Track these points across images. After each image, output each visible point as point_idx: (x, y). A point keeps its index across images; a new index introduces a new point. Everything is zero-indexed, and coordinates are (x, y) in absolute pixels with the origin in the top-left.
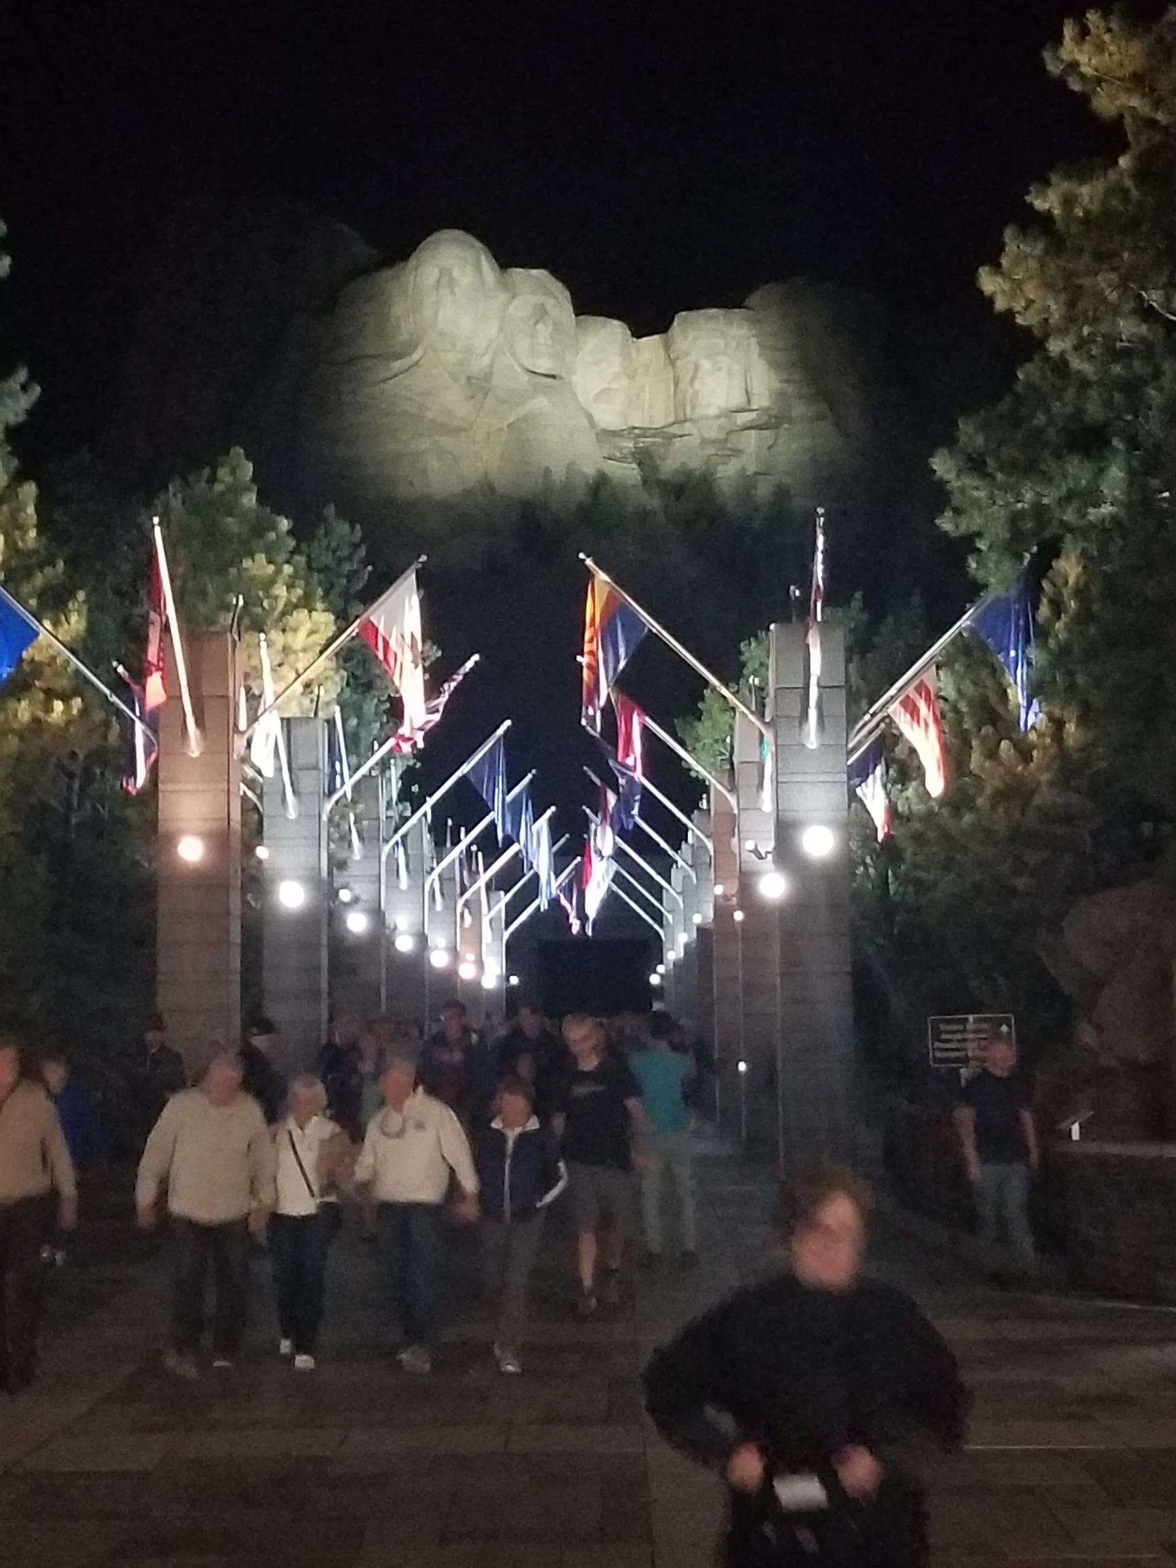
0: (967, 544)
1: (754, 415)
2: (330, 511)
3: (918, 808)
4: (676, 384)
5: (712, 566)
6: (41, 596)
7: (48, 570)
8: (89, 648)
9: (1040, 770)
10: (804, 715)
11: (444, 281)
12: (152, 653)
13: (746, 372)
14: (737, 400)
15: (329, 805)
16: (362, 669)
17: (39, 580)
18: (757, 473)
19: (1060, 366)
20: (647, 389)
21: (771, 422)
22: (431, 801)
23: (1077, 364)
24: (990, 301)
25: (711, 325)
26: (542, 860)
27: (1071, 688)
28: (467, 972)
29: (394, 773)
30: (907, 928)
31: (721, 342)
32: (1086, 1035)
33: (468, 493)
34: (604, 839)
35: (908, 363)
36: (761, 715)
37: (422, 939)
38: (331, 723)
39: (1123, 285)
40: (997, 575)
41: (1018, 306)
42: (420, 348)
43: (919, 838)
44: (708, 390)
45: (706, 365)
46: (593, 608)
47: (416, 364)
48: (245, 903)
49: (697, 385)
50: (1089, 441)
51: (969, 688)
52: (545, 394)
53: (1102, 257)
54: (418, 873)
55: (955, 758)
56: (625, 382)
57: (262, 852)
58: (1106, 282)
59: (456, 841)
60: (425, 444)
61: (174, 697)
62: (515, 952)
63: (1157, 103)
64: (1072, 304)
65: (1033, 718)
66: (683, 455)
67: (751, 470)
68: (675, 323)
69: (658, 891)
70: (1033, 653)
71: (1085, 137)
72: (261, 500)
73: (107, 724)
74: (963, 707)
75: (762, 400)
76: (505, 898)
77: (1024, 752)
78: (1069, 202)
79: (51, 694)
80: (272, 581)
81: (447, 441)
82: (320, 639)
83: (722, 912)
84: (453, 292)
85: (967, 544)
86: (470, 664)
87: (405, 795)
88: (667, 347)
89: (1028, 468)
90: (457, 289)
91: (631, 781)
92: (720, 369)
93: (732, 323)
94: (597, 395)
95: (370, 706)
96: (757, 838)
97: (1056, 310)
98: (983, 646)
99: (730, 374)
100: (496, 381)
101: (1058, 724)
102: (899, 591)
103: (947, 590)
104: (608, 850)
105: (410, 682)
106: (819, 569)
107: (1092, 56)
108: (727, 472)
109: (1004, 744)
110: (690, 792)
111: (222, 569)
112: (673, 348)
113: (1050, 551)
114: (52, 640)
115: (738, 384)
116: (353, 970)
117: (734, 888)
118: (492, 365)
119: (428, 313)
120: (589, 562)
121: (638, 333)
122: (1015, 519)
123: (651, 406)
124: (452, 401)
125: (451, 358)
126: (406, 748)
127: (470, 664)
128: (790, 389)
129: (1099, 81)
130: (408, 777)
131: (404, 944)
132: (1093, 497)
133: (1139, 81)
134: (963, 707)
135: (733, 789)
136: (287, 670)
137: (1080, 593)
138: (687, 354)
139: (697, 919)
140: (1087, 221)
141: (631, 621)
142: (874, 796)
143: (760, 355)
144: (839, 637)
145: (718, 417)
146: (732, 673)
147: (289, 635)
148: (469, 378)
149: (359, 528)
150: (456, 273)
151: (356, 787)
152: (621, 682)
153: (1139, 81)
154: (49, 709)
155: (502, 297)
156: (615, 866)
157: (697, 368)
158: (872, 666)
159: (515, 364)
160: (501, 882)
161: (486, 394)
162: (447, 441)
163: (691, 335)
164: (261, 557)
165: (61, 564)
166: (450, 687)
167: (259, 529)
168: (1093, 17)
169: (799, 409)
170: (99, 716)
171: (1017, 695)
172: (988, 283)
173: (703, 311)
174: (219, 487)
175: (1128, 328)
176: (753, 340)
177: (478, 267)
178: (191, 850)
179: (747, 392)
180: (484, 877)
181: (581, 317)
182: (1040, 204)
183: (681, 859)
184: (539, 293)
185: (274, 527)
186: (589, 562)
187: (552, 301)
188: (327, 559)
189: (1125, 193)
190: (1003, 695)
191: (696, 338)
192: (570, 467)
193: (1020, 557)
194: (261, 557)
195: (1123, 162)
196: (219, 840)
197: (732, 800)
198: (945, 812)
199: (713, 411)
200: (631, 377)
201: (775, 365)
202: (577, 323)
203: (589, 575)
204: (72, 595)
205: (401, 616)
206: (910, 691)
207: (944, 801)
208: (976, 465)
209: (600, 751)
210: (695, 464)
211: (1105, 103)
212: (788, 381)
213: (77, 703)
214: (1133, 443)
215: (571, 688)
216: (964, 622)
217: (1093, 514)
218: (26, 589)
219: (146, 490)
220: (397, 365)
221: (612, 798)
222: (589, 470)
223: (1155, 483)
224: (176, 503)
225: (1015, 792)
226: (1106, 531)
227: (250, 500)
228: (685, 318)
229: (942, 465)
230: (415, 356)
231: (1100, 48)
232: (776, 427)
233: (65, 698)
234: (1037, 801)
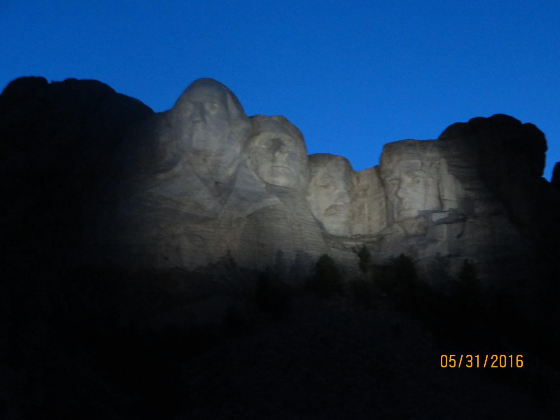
4: (387, 198)
13: (438, 184)
14: (432, 204)
18: (449, 256)
31: (417, 162)
45: (407, 180)
52: (278, 196)
56: (348, 200)
67: (445, 252)
75: (451, 203)
84: (204, 120)
90: (208, 119)
94: (327, 210)
99: (426, 185)
108: (426, 254)
115: (432, 191)
118: (235, 174)
119: (185, 137)
123: (369, 219)
124: (204, 197)
125: (203, 169)
128: (472, 194)
138: (392, 172)
143: (449, 171)
145: (417, 218)
148: (217, 183)
150: (207, 107)
157: (400, 180)
159: (255, 175)
169: (479, 209)
176: (443, 161)
187: (288, 137)
191: (399, 160)
199: (414, 213)
200: (354, 199)
201: (460, 178)
212: (469, 189)
220: (162, 176)
222: (315, 253)
232: (464, 220)
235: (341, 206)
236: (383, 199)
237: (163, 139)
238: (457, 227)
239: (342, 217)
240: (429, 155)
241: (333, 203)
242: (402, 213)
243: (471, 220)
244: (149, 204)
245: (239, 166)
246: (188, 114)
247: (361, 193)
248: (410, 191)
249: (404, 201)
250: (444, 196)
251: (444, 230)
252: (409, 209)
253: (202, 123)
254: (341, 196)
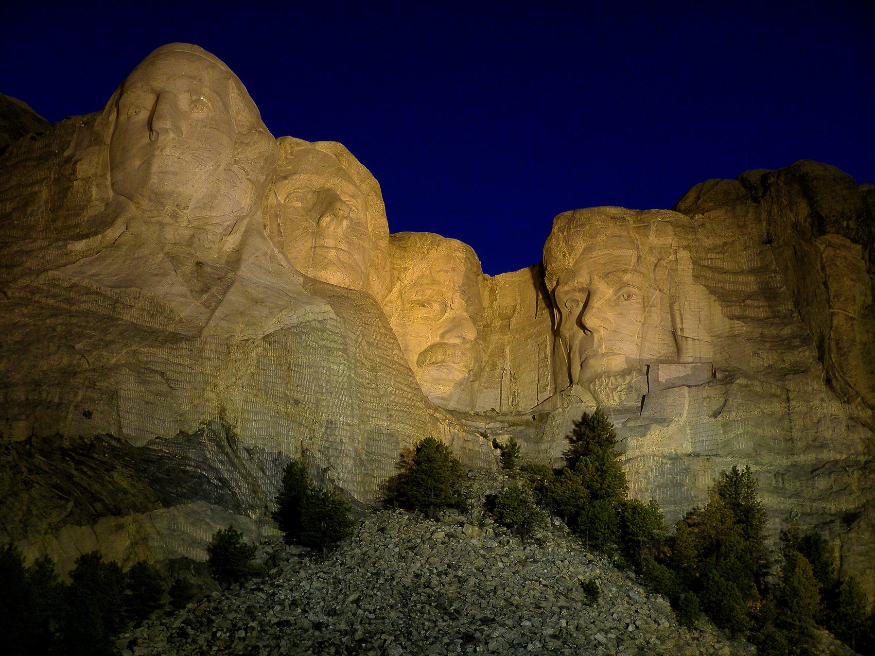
1: (688, 370)
4: (556, 333)
11: (164, 107)
13: (671, 306)
14: (656, 345)
20: (507, 351)
25: (613, 229)
31: (630, 254)
42: (120, 221)
45: (605, 291)
47: (114, 245)
49: (590, 321)
52: (332, 304)
56: (471, 334)
68: (555, 230)
75: (700, 349)
84: (177, 129)
92: (629, 296)
93: (647, 227)
99: (646, 305)
100: (245, 271)
112: (549, 268)
115: (658, 317)
118: (239, 251)
121: (493, 263)
125: (169, 235)
138: (572, 273)
143: (696, 277)
145: (624, 373)
148: (199, 264)
155: (264, 143)
159: (280, 256)
161: (229, 287)
163: (580, 245)
173: (602, 208)
176: (684, 254)
177: (221, 94)
179: (674, 334)
181: (398, 235)
191: (588, 249)
199: (617, 363)
200: (484, 333)
202: (392, 240)
212: (738, 318)
220: (80, 246)
228: (570, 220)
230: (111, 234)
235: (454, 345)
236: (548, 337)
237: (84, 169)
239: (457, 371)
240: (653, 239)
241: (438, 339)
242: (592, 362)
243: (742, 381)
244: (51, 302)
245: (247, 233)
246: (144, 115)
247: (497, 323)
248: (610, 315)
249: (596, 336)
250: (682, 329)
252: (607, 354)
253: (172, 135)
254: (455, 325)
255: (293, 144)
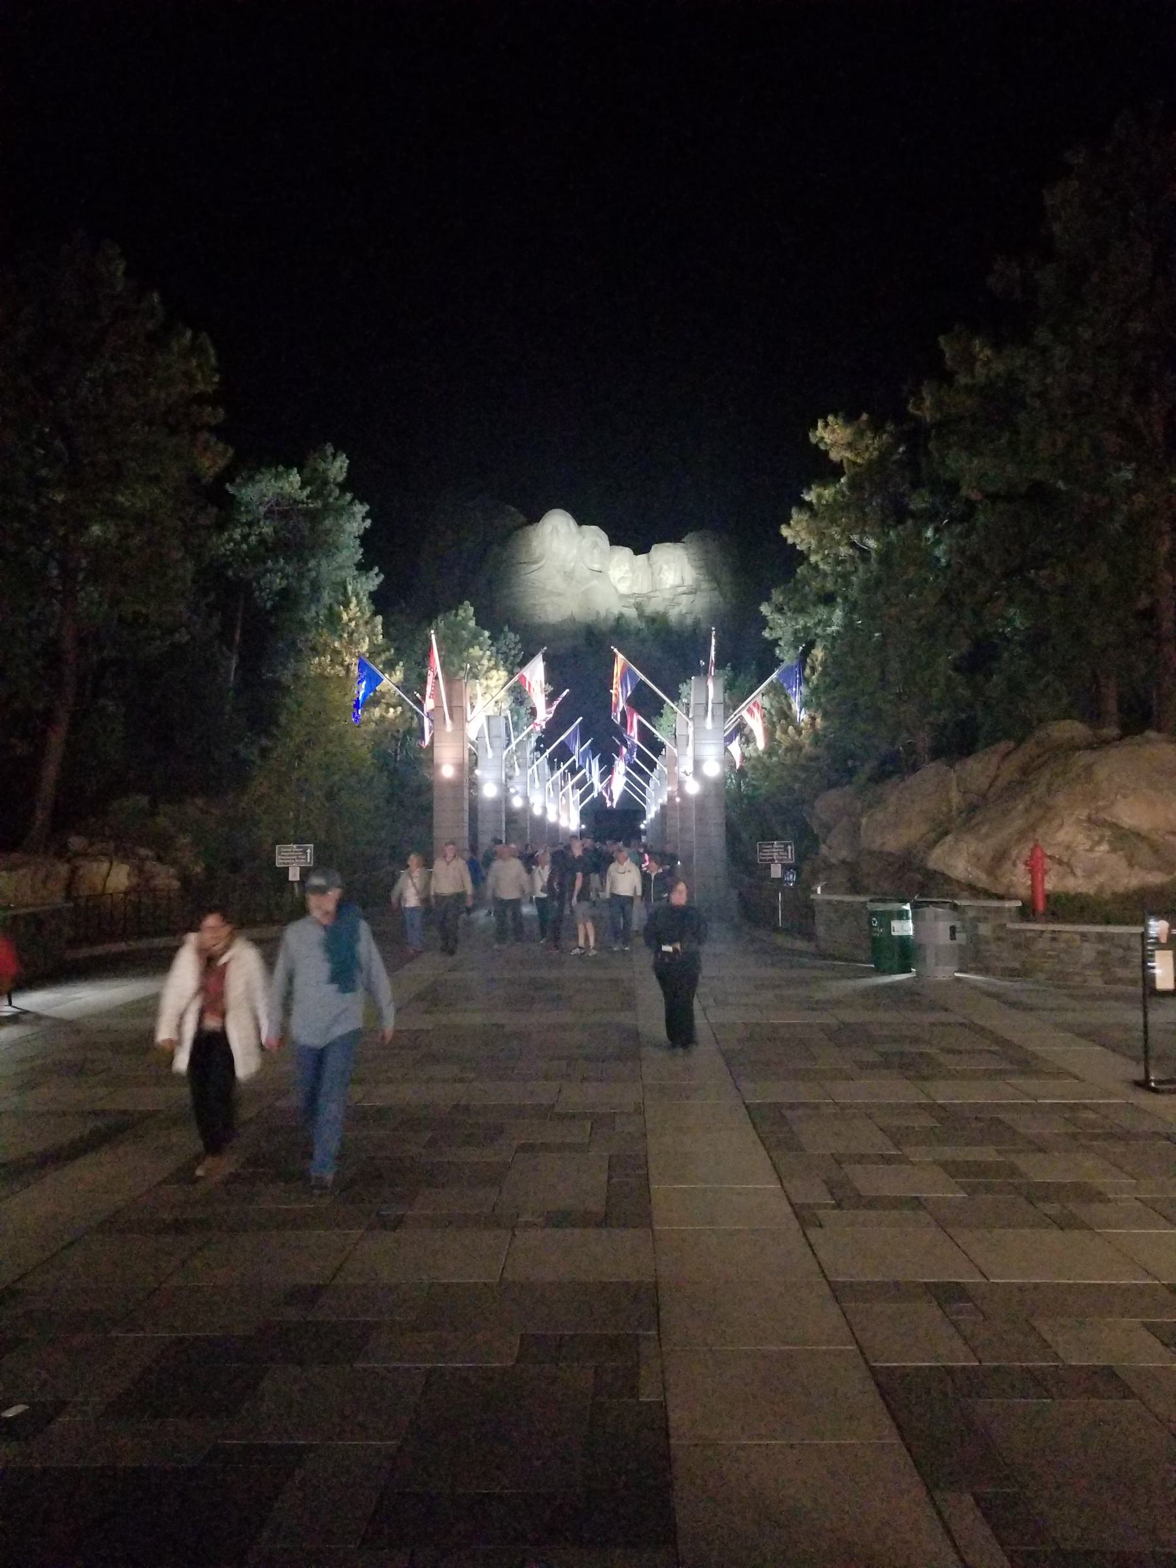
0: (775, 643)
2: (506, 628)
3: (754, 755)
5: (669, 653)
6: (384, 663)
7: (387, 654)
8: (405, 686)
9: (805, 739)
10: (707, 711)
12: (429, 689)
14: (678, 581)
15: (505, 753)
16: (519, 695)
17: (383, 657)
19: (816, 567)
21: (693, 592)
22: (548, 751)
23: (822, 566)
24: (785, 539)
26: (595, 777)
27: (819, 705)
28: (563, 823)
29: (533, 739)
30: (753, 809)
32: (824, 849)
33: (564, 621)
34: (620, 767)
35: (753, 564)
36: (687, 714)
37: (545, 809)
38: (506, 718)
39: (843, 532)
40: (788, 656)
41: (798, 541)
43: (754, 767)
44: (667, 578)
45: (665, 567)
46: (617, 669)
48: (470, 794)
50: (828, 599)
51: (775, 703)
53: (833, 521)
54: (544, 781)
55: (770, 734)
57: (477, 772)
58: (835, 531)
59: (559, 768)
60: (543, 600)
61: (439, 707)
62: (583, 814)
63: (857, 455)
64: (820, 541)
65: (803, 716)
66: (654, 606)
69: (644, 789)
70: (803, 689)
71: (827, 470)
72: (477, 624)
73: (412, 718)
74: (773, 712)
76: (579, 792)
77: (799, 731)
78: (819, 497)
79: (388, 705)
80: (482, 658)
81: (556, 599)
82: (502, 682)
83: (671, 798)
85: (775, 643)
86: (565, 693)
87: (537, 749)
88: (649, 558)
89: (801, 610)
91: (633, 743)
95: (523, 711)
96: (687, 765)
97: (814, 543)
98: (782, 686)
99: (675, 571)
101: (813, 719)
102: (747, 662)
103: (766, 661)
104: (623, 772)
105: (538, 698)
106: (713, 653)
107: (831, 435)
108: (673, 614)
109: (791, 728)
110: (657, 748)
111: (461, 652)
113: (811, 645)
114: (389, 683)
115: (678, 574)
116: (515, 821)
117: (676, 788)
120: (615, 650)
122: (796, 632)
124: (556, 582)
126: (538, 729)
127: (565, 693)
128: (701, 577)
129: (833, 445)
130: (539, 740)
131: (537, 811)
132: (828, 623)
133: (850, 446)
134: (773, 712)
135: (676, 746)
136: (487, 696)
137: (824, 664)
139: (660, 801)
140: (828, 505)
141: (633, 676)
142: (735, 748)
144: (721, 681)
146: (675, 697)
147: (489, 682)
149: (517, 635)
151: (517, 745)
152: (629, 701)
153: (850, 446)
154: (387, 712)
156: (625, 779)
158: (736, 693)
160: (579, 785)
162: (556, 599)
164: (477, 648)
165: (392, 651)
166: (556, 703)
167: (476, 636)
168: (830, 418)
169: (704, 586)
170: (409, 714)
171: (796, 707)
172: (785, 531)
174: (459, 618)
175: (844, 551)
177: (569, 525)
178: (447, 771)
180: (570, 783)
182: (807, 498)
183: (654, 776)
184: (595, 535)
185: (482, 635)
186: (615, 650)
188: (504, 649)
189: (844, 496)
190: (790, 707)
192: (607, 610)
193: (797, 648)
194: (477, 648)
195: (843, 480)
196: (460, 767)
197: (675, 751)
198: (765, 756)
200: (633, 572)
203: (615, 655)
204: (397, 664)
205: (535, 672)
206: (751, 705)
207: (764, 752)
208: (780, 610)
209: (619, 731)
210: (661, 609)
211: (834, 455)
213: (399, 709)
214: (845, 599)
215: (607, 705)
216: (774, 676)
217: (829, 630)
218: (378, 660)
219: (429, 618)
220: (535, 567)
221: (624, 750)
222: (616, 612)
223: (855, 617)
224: (441, 624)
225: (795, 748)
226: (834, 638)
227: (472, 623)
229: (765, 609)
231: (833, 431)
233: (394, 707)
234: (804, 751)
238: (691, 596)
239: (628, 583)
251: (685, 599)
254: (627, 572)
255: (584, 527)
